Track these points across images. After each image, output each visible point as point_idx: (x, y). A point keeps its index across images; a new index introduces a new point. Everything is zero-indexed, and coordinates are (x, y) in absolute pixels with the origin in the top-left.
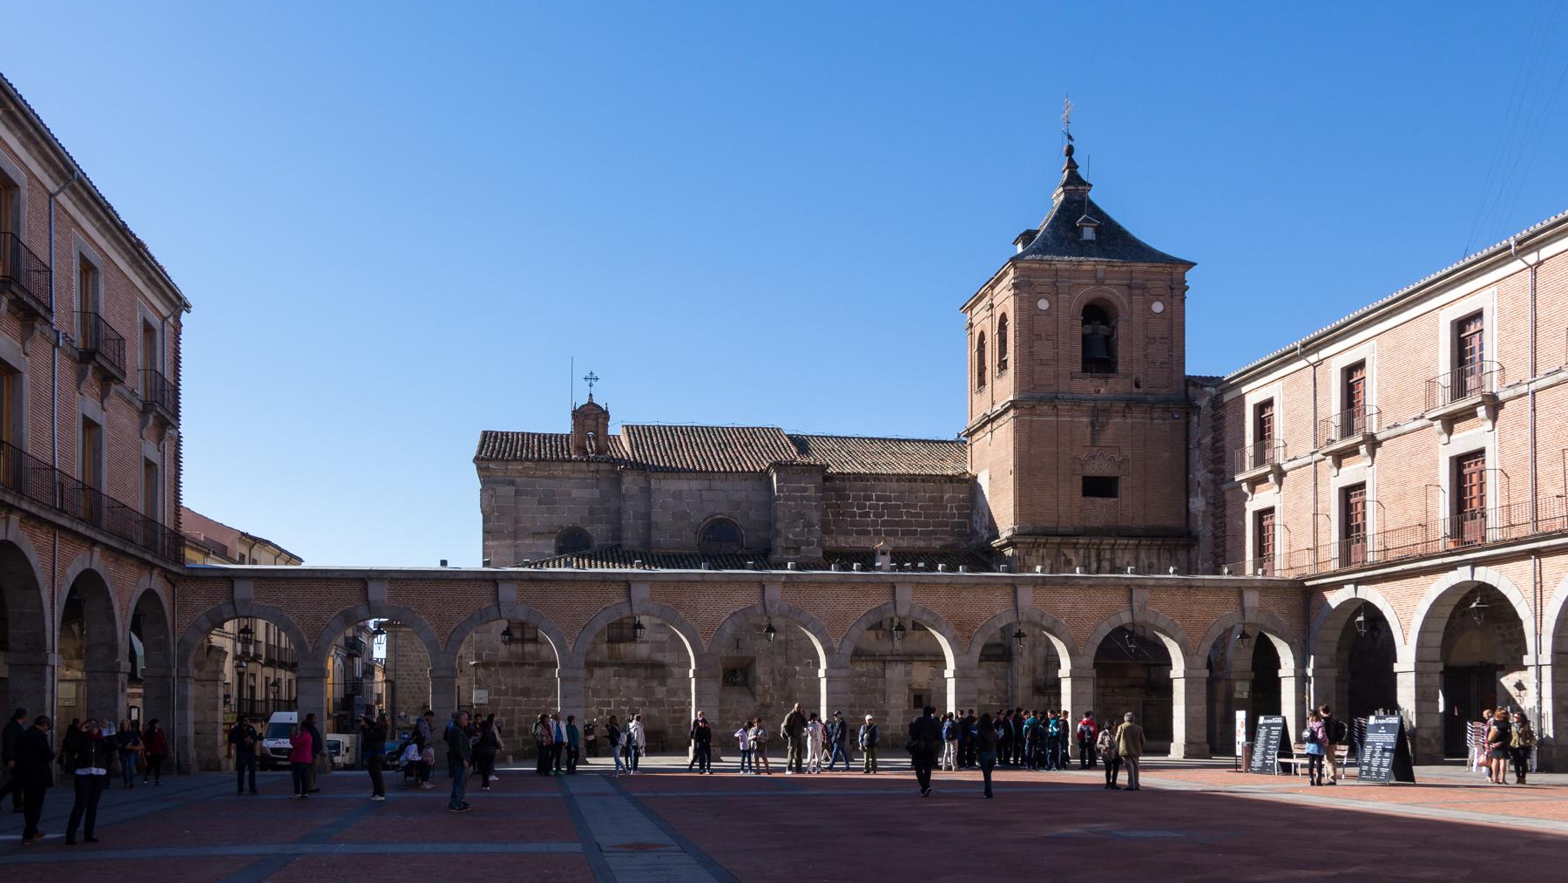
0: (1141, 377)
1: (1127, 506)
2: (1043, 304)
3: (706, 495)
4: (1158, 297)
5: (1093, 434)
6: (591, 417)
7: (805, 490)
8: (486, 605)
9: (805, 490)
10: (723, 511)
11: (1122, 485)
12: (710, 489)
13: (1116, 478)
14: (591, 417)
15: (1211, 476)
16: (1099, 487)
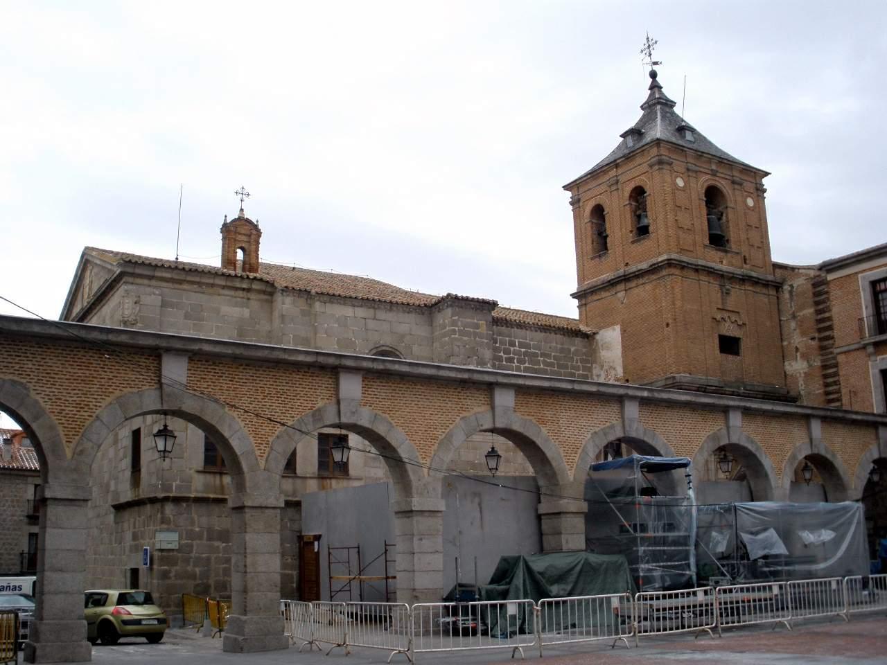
0: (747, 257)
1: (746, 365)
2: (680, 183)
3: (371, 324)
4: (750, 194)
5: (722, 299)
6: (241, 233)
7: (477, 326)
8: (320, 404)
9: (477, 326)
10: (387, 341)
11: (743, 346)
12: (375, 319)
13: (739, 339)
14: (241, 233)
15: (813, 343)
16: (729, 345)
